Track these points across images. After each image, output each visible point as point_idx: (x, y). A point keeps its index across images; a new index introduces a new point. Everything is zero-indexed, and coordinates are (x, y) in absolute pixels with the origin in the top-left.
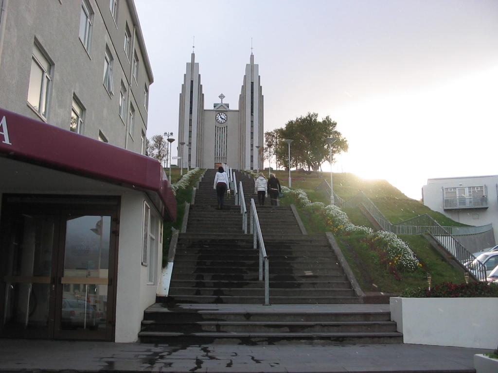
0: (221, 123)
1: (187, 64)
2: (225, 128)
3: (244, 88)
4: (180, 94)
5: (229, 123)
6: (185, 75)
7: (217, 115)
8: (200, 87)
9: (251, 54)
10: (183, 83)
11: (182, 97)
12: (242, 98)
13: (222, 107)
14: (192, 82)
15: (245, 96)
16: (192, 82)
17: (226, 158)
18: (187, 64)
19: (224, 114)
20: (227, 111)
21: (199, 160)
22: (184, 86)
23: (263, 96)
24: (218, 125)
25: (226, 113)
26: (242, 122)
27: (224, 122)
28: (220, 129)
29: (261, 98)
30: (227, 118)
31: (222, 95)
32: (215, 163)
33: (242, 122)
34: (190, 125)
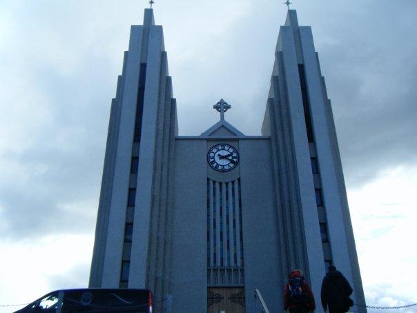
0: (223, 171)
1: (134, 28)
2: (233, 182)
3: (278, 82)
4: (113, 100)
5: (244, 170)
6: (126, 53)
7: (210, 151)
8: (166, 83)
9: (282, 20)
10: (121, 74)
11: (116, 105)
12: (277, 107)
13: (222, 130)
14: (143, 67)
15: (286, 97)
16: (143, 67)
17: (242, 270)
18: (134, 29)
19: (230, 147)
20: (237, 140)
21: (156, 279)
22: (122, 81)
23: (329, 100)
24: (215, 176)
25: (234, 144)
26: (283, 164)
27: (231, 169)
28: (222, 187)
29: (327, 103)
30: (238, 157)
31: (222, 102)
32: (208, 288)
33: (283, 164)
34: (134, 169)
